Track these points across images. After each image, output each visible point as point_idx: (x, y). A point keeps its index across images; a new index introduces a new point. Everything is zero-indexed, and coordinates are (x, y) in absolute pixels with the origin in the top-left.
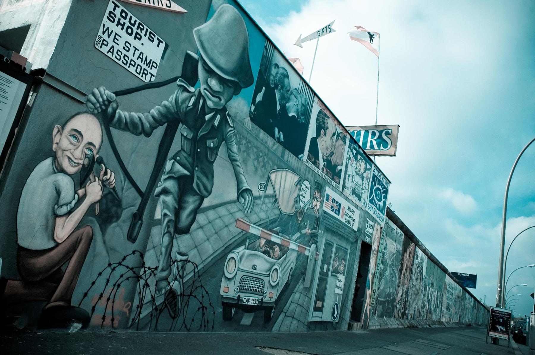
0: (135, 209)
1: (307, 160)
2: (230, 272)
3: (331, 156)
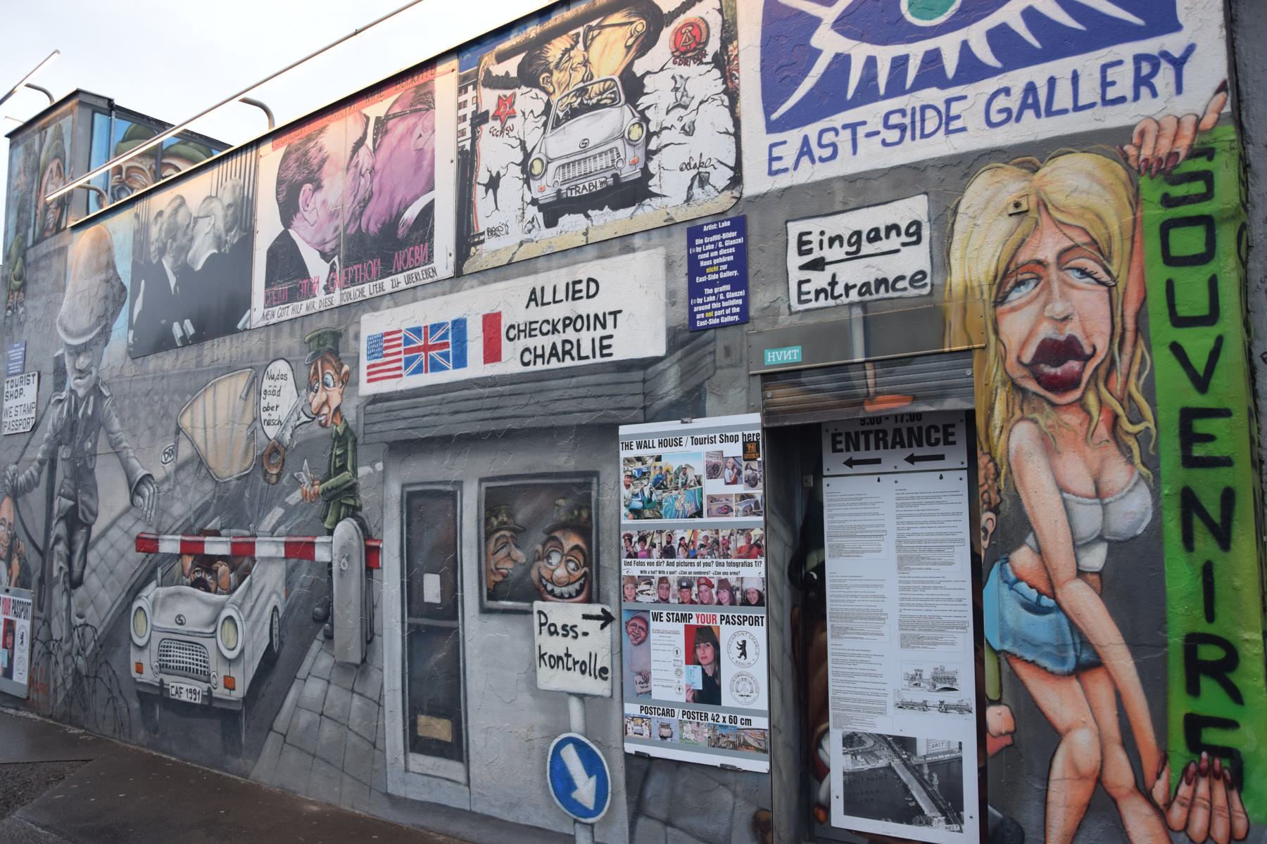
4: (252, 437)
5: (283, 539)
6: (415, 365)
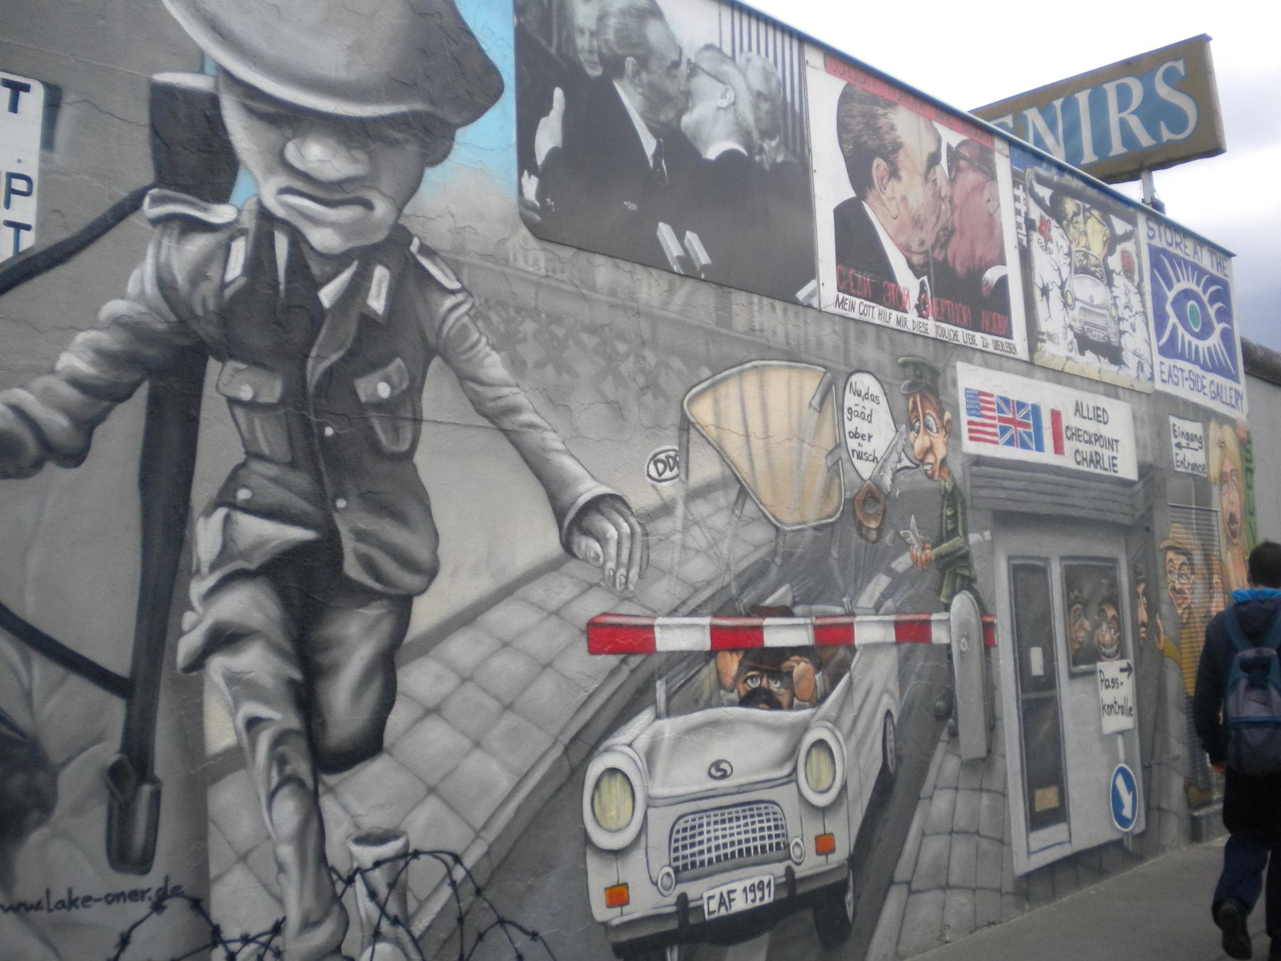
0: (109, 751)
1: (841, 295)
2: (614, 827)
3: (945, 245)
4: (834, 470)
5: (893, 618)
6: (1007, 436)
